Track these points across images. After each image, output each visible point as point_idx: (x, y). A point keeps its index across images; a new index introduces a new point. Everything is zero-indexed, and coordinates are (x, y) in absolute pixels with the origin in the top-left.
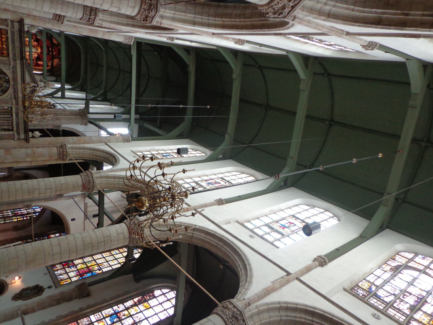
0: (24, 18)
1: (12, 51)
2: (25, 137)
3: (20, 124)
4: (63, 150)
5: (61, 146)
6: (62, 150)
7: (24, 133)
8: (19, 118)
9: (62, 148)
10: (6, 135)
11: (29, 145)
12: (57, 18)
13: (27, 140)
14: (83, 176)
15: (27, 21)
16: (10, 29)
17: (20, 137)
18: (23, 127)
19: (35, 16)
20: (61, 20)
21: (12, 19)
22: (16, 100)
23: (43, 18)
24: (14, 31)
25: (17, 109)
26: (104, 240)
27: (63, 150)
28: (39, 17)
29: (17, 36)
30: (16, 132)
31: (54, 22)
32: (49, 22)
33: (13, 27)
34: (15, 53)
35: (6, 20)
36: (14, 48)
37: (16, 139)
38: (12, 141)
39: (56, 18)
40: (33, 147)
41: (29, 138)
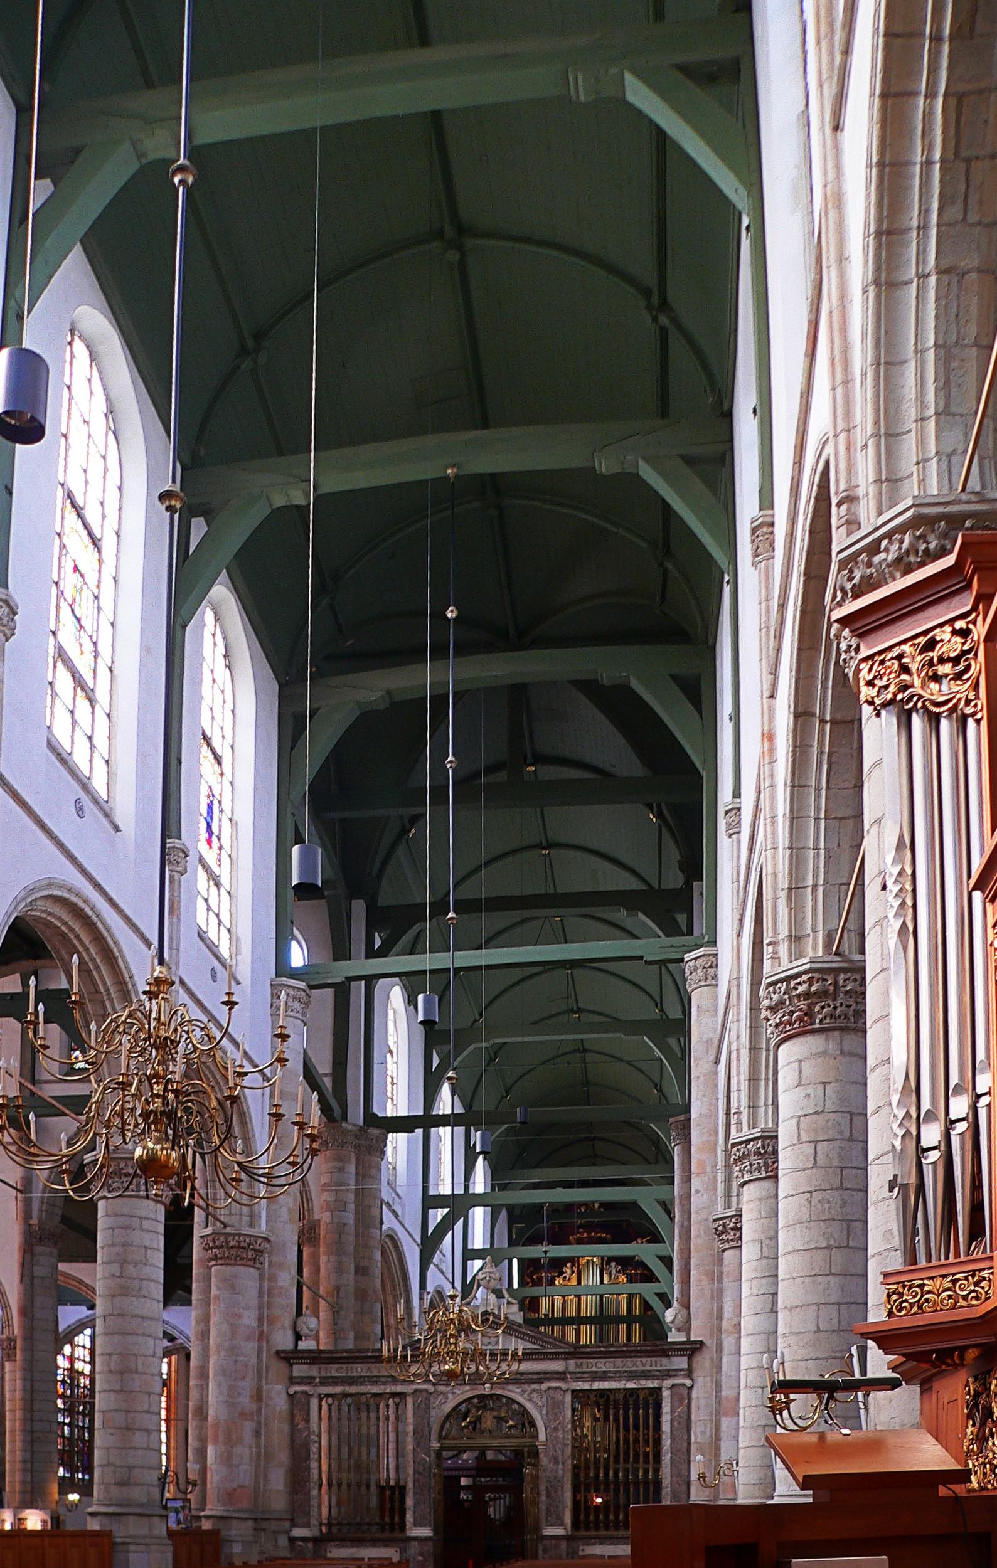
0: (274, 1350)
1: (384, 1383)
2: (684, 1355)
3: (635, 1369)
4: (732, 1229)
5: (719, 1235)
6: (732, 1233)
7: (668, 1356)
8: (610, 1372)
9: (722, 1233)
10: (672, 1412)
11: (710, 1342)
12: (250, 1256)
13: (693, 1349)
14: (743, 1175)
15: (283, 1340)
16: (316, 1385)
17: (682, 1370)
18: (644, 1360)
19: (260, 1320)
20: (252, 1241)
21: (287, 1381)
22: (548, 1379)
23: (260, 1296)
24: (320, 1378)
25: (579, 1375)
26: (810, 1142)
27: (732, 1229)
28: (260, 1307)
29: (333, 1371)
30: (663, 1380)
31: (270, 1263)
32: (273, 1278)
33: (309, 1381)
34: (388, 1377)
35: (291, 1397)
36: (374, 1379)
37: (688, 1382)
38: (694, 1394)
39: (250, 1260)
40: (719, 1329)
41: (688, 1342)
